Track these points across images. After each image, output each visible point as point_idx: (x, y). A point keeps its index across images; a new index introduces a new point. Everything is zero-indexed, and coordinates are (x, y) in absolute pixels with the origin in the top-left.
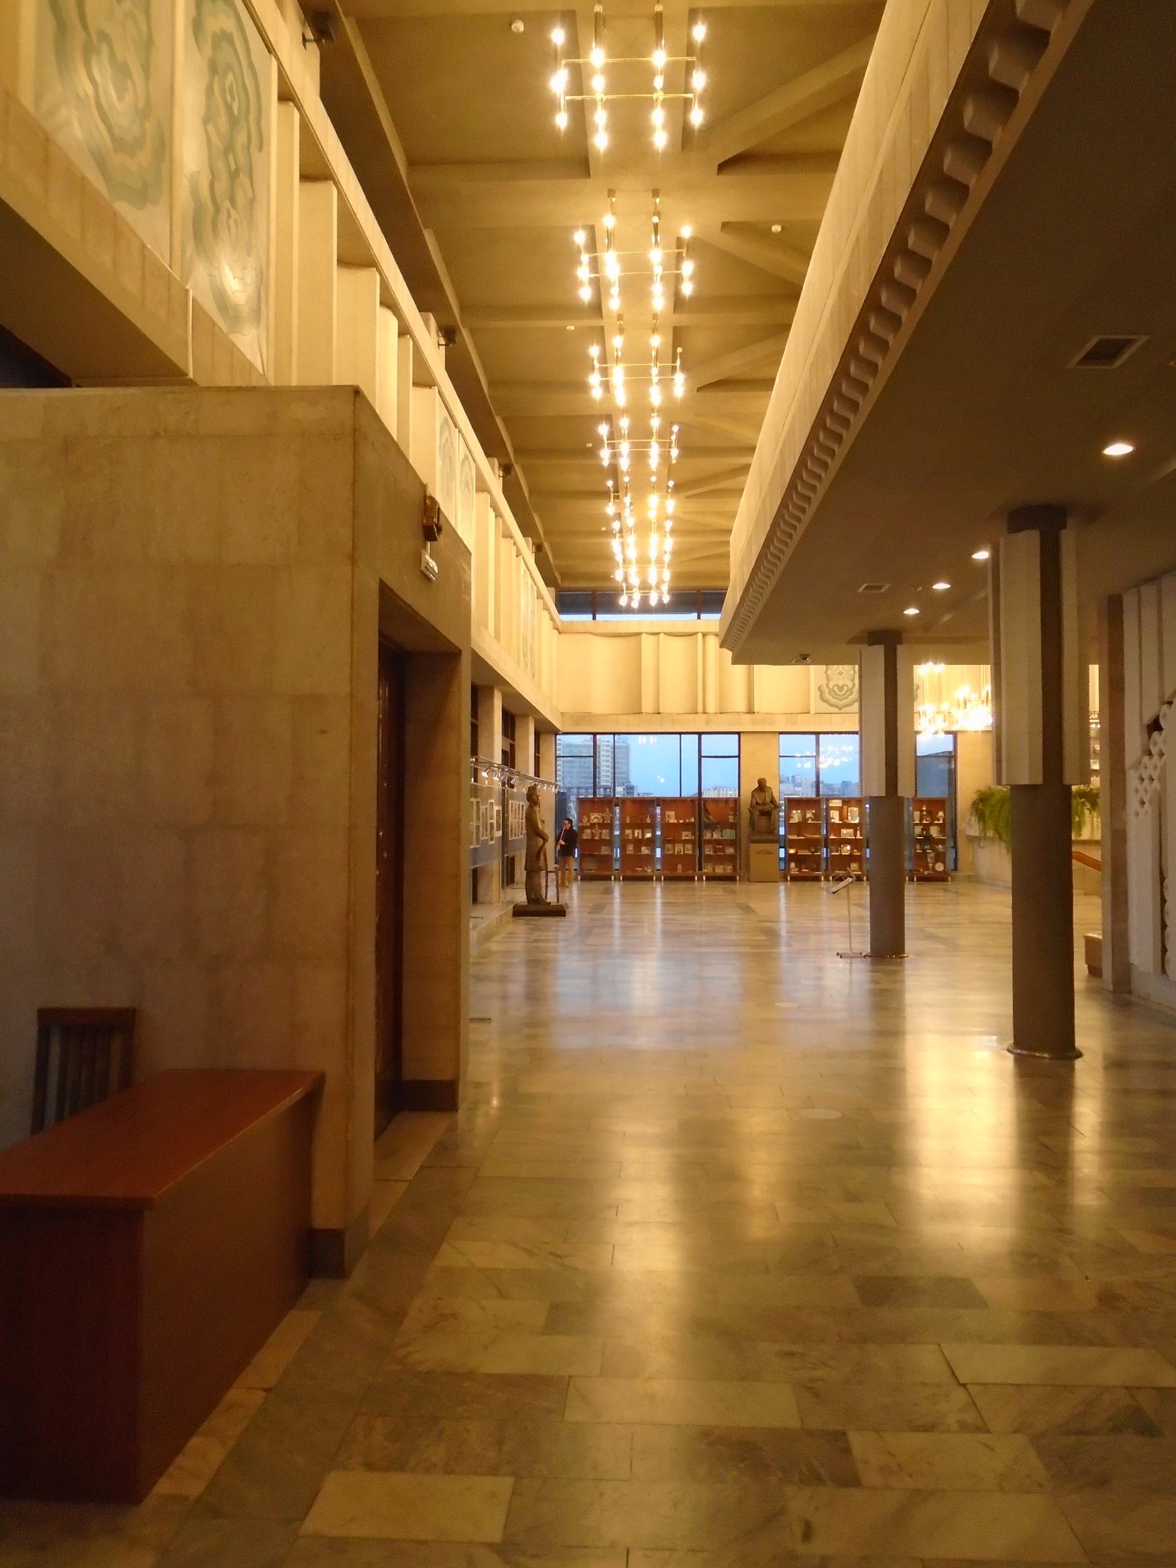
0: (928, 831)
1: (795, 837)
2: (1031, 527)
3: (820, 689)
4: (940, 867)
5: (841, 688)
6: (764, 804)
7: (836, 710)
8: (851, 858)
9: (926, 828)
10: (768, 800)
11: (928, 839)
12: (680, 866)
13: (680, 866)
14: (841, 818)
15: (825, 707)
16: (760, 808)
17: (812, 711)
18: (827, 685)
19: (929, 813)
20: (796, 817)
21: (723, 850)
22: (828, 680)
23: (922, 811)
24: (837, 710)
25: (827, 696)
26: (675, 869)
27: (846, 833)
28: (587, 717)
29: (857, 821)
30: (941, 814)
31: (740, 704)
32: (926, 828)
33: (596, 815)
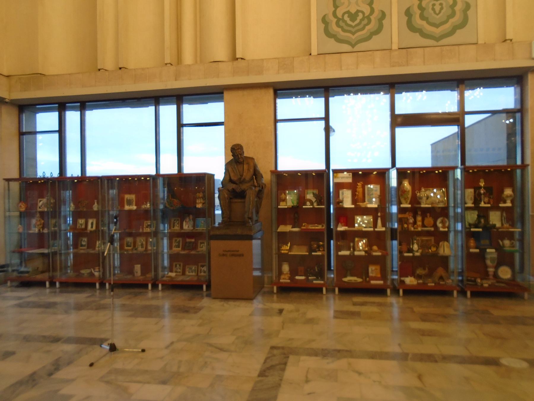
0: (487, 218)
1: (288, 228)
2: (512, 86)
3: (324, 20)
4: (505, 273)
5: (353, 17)
6: (241, 181)
7: (346, 47)
8: (369, 259)
9: (483, 214)
10: (247, 175)
11: (489, 228)
12: (138, 268)
13: (138, 268)
14: (354, 201)
15: (332, 45)
16: (232, 186)
17: (314, 52)
18: (334, 14)
19: (489, 190)
20: (290, 199)
21: (194, 247)
22: (336, 7)
23: (477, 188)
25: (334, 28)
26: (131, 272)
27: (362, 222)
28: (37, 78)
29: (375, 206)
30: (508, 192)
31: (220, 52)
32: (483, 214)
33: (44, 200)
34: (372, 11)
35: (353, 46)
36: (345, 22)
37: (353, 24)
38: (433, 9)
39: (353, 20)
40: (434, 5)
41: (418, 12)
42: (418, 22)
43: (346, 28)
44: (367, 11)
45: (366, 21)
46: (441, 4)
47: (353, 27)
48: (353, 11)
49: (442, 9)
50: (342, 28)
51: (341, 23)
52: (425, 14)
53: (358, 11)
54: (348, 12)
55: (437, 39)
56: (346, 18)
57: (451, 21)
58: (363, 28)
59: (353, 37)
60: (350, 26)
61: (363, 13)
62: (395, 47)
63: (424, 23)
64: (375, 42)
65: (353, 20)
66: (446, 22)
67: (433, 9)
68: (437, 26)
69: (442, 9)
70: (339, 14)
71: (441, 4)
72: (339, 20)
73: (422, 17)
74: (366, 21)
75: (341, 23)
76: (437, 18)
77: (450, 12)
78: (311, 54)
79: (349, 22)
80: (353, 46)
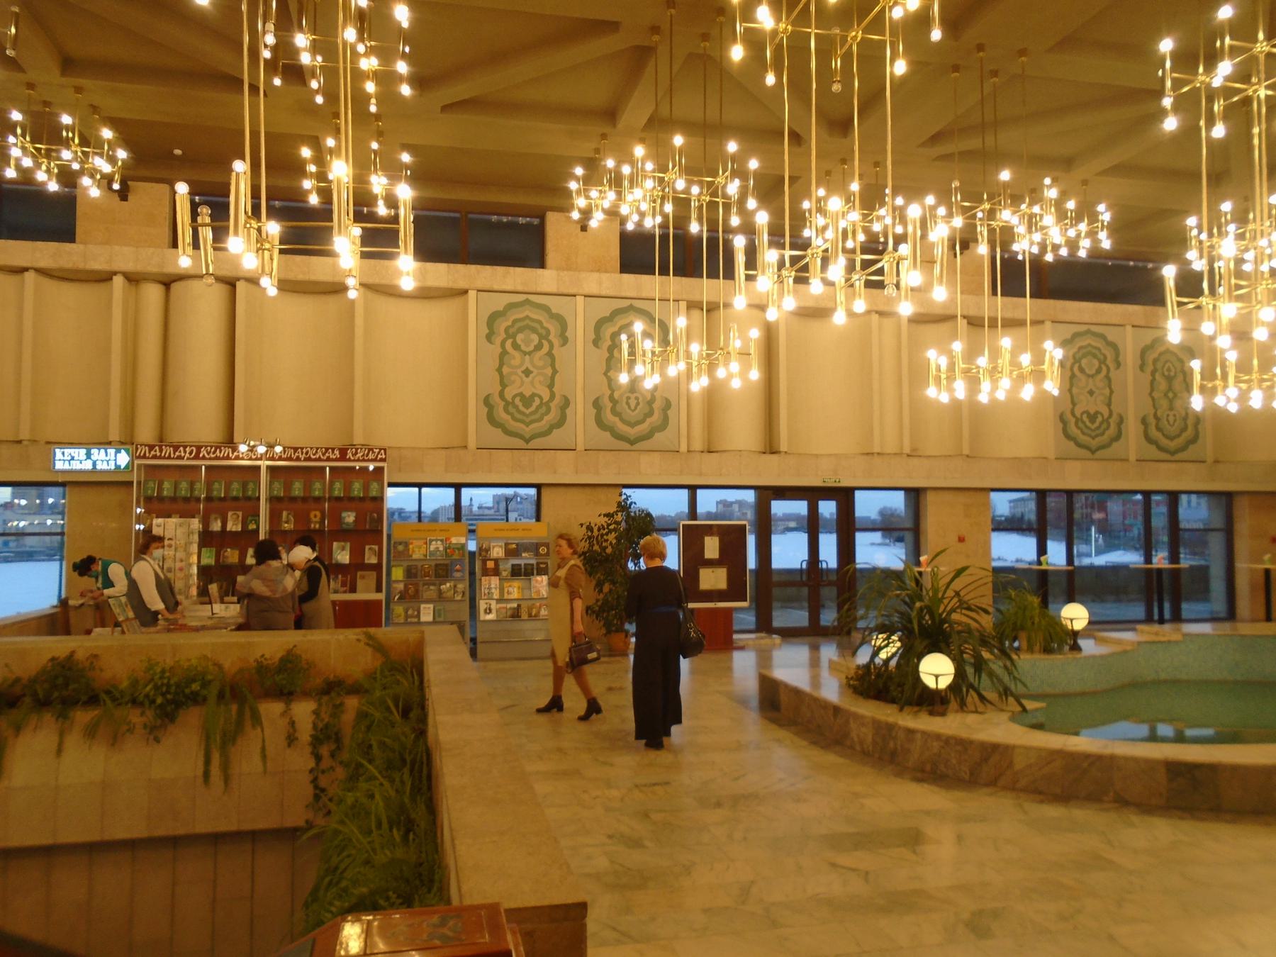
3: (487, 401)
5: (527, 401)
15: (497, 436)
17: (472, 444)
22: (503, 385)
24: (521, 444)
25: (501, 414)
34: (553, 396)
35: (527, 441)
36: (516, 407)
37: (527, 412)
38: (628, 403)
39: (527, 405)
40: (628, 398)
41: (610, 405)
42: (609, 417)
43: (518, 416)
44: (546, 397)
45: (544, 409)
46: (637, 398)
47: (527, 416)
48: (527, 394)
49: (638, 404)
50: (512, 415)
51: (511, 409)
52: (618, 408)
53: (534, 395)
54: (521, 395)
55: (632, 443)
56: (517, 400)
57: (649, 420)
58: (540, 419)
59: (527, 429)
60: (523, 414)
61: (540, 397)
62: (580, 447)
63: (617, 419)
64: (556, 438)
65: (527, 405)
66: (643, 421)
67: (628, 403)
68: (632, 425)
69: (638, 404)
70: (508, 396)
71: (637, 398)
72: (507, 404)
73: (614, 412)
74: (544, 409)
75: (511, 409)
76: (632, 416)
77: (647, 411)
78: (466, 447)
79: (521, 408)
80: (527, 441)
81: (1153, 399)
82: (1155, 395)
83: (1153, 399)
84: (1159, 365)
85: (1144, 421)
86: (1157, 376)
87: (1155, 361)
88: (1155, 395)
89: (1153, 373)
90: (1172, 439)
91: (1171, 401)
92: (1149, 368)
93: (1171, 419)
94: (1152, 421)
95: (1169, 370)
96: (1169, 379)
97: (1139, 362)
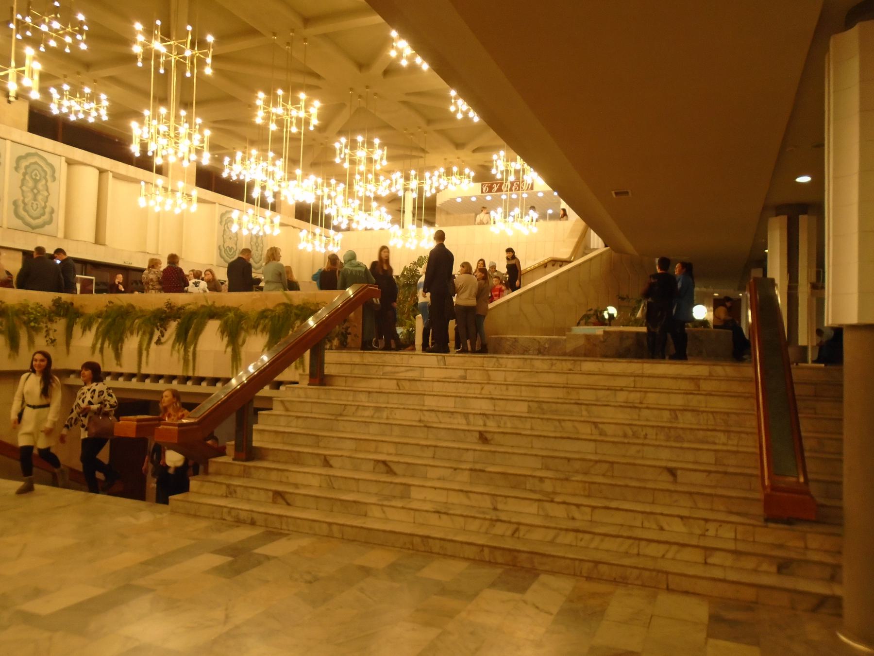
81: (23, 191)
82: (24, 188)
83: (23, 191)
84: (29, 170)
85: (15, 203)
86: (27, 177)
87: (27, 167)
88: (24, 188)
89: (25, 174)
90: (34, 218)
91: (35, 195)
92: (22, 171)
93: (35, 207)
94: (21, 205)
95: (36, 175)
96: (36, 181)
97: (15, 165)
